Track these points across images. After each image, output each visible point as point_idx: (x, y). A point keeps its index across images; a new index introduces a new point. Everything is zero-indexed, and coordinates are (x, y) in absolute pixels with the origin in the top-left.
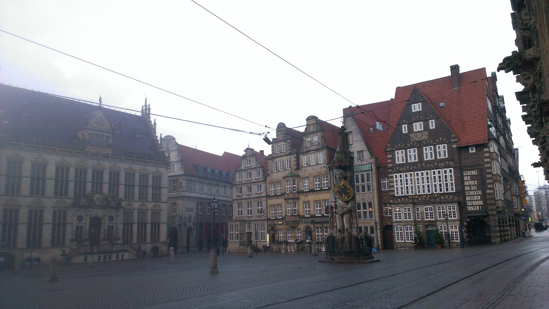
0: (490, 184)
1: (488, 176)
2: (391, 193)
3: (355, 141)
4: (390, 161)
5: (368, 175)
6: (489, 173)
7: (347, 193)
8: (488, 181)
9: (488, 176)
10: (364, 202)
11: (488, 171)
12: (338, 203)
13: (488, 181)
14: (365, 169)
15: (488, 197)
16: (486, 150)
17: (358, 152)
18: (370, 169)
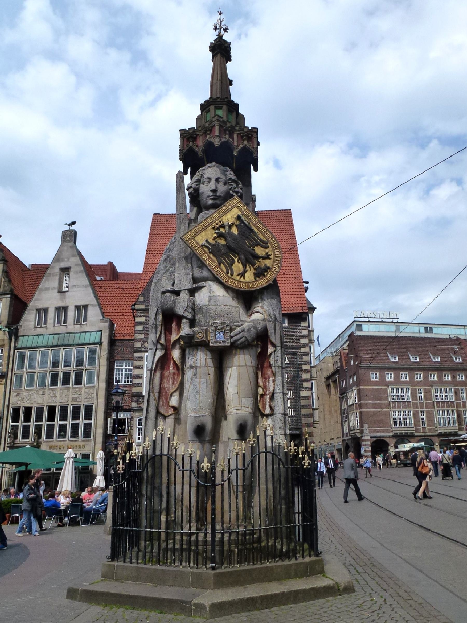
0: (307, 380)
1: (304, 367)
2: (135, 390)
3: (75, 286)
4: (140, 328)
5: (92, 352)
6: (306, 363)
7: (257, 257)
8: (304, 376)
9: (304, 367)
10: (76, 404)
11: (305, 358)
12: (202, 298)
13: (304, 376)
14: (87, 341)
15: (303, 402)
16: (303, 324)
17: (78, 308)
18: (97, 340)
